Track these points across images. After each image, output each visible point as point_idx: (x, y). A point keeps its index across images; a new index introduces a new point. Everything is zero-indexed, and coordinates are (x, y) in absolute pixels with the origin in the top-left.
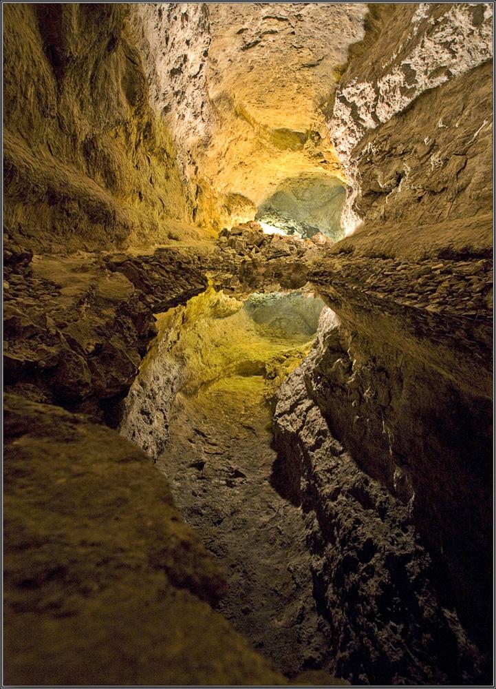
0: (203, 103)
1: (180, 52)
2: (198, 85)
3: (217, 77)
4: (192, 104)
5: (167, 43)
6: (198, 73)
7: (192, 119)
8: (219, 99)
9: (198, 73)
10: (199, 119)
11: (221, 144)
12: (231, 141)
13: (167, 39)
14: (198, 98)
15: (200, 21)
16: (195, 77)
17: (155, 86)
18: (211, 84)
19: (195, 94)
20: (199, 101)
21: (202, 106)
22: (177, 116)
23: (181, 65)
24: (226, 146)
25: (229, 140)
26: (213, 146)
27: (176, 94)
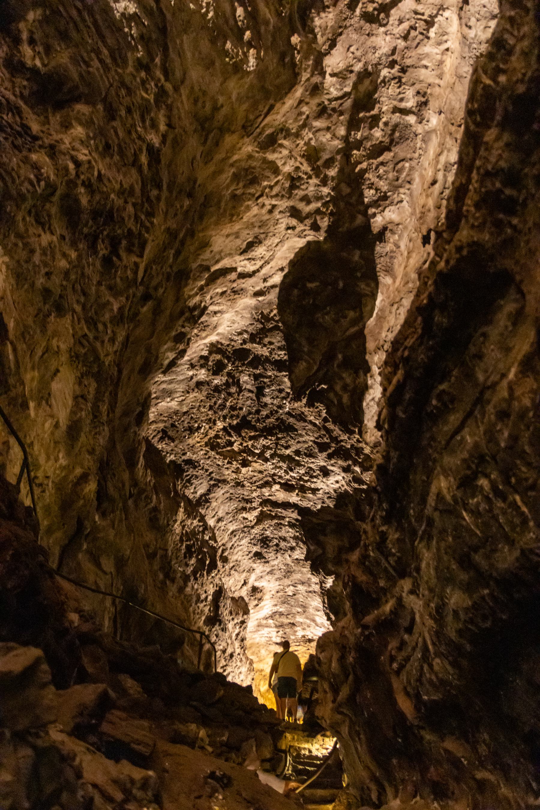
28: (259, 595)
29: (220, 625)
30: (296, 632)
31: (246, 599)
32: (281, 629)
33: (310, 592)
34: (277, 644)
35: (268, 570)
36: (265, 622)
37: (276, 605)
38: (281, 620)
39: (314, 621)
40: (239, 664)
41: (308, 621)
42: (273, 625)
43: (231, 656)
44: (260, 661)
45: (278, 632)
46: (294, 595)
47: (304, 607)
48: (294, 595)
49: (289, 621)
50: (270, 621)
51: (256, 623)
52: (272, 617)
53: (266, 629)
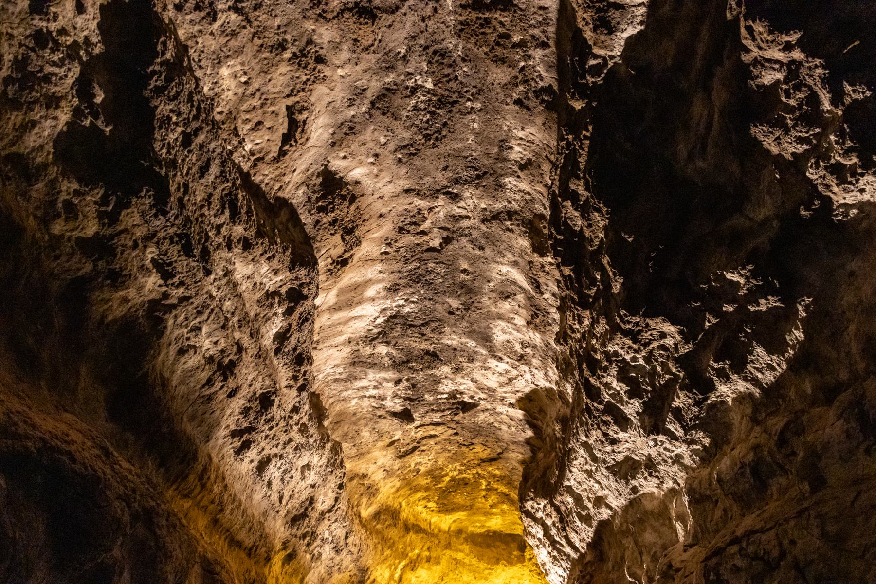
0: (347, 533)
1: (303, 497)
2: (333, 519)
3: (371, 491)
4: (331, 539)
5: (281, 502)
6: (334, 506)
7: (333, 554)
8: (377, 515)
9: (334, 506)
10: (345, 552)
11: (387, 574)
12: (405, 566)
13: (281, 499)
14: (339, 530)
15: (328, 461)
16: (330, 511)
17: (264, 549)
18: (364, 500)
19: (334, 526)
20: (340, 532)
21: (346, 537)
22: (308, 556)
23: (306, 509)
24: (397, 576)
25: (401, 566)
26: (374, 580)
27: (304, 536)
28: (344, 211)
29: (160, 206)
30: (438, 382)
31: (307, 219)
32: (406, 375)
33: (496, 217)
34: (395, 414)
35: (375, 86)
36: (368, 350)
37: (393, 289)
38: (405, 342)
39: (486, 339)
40: (298, 438)
41: (472, 343)
42: (387, 361)
43: (266, 401)
44: (360, 455)
45: (398, 382)
46: (447, 241)
47: (469, 291)
48: (447, 241)
49: (425, 346)
50: (383, 349)
51: (346, 352)
52: (383, 335)
53: (371, 374)
